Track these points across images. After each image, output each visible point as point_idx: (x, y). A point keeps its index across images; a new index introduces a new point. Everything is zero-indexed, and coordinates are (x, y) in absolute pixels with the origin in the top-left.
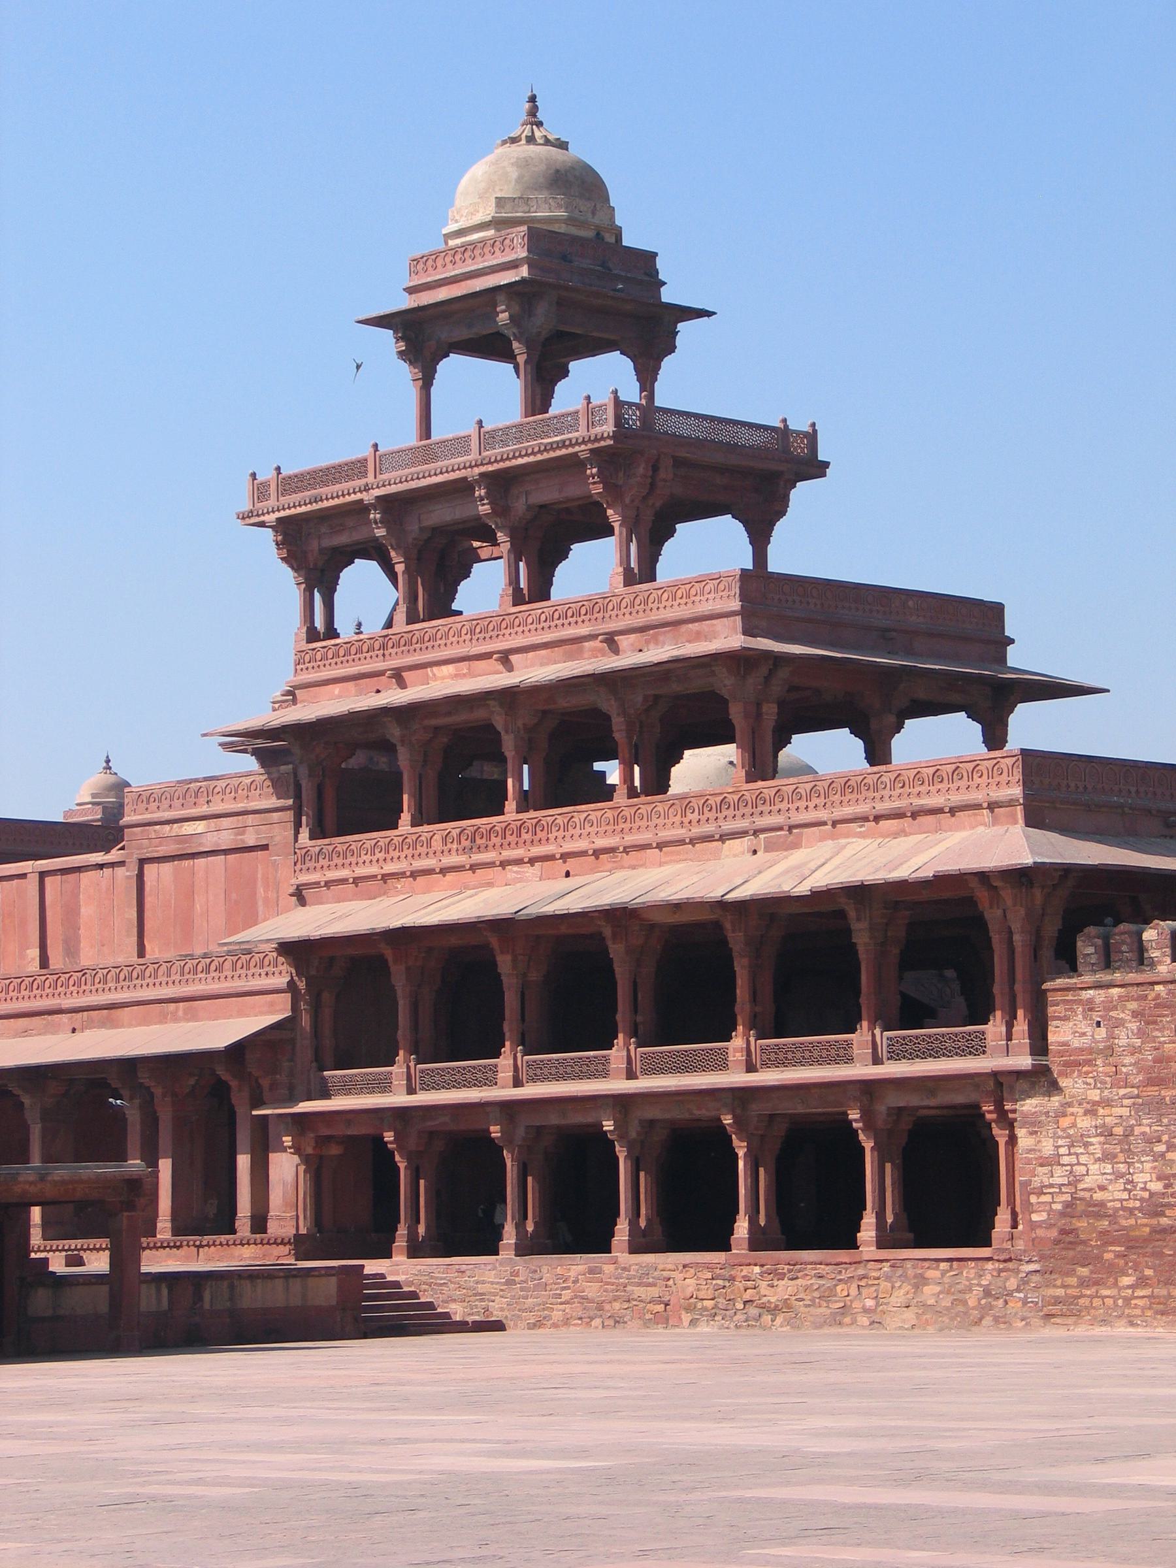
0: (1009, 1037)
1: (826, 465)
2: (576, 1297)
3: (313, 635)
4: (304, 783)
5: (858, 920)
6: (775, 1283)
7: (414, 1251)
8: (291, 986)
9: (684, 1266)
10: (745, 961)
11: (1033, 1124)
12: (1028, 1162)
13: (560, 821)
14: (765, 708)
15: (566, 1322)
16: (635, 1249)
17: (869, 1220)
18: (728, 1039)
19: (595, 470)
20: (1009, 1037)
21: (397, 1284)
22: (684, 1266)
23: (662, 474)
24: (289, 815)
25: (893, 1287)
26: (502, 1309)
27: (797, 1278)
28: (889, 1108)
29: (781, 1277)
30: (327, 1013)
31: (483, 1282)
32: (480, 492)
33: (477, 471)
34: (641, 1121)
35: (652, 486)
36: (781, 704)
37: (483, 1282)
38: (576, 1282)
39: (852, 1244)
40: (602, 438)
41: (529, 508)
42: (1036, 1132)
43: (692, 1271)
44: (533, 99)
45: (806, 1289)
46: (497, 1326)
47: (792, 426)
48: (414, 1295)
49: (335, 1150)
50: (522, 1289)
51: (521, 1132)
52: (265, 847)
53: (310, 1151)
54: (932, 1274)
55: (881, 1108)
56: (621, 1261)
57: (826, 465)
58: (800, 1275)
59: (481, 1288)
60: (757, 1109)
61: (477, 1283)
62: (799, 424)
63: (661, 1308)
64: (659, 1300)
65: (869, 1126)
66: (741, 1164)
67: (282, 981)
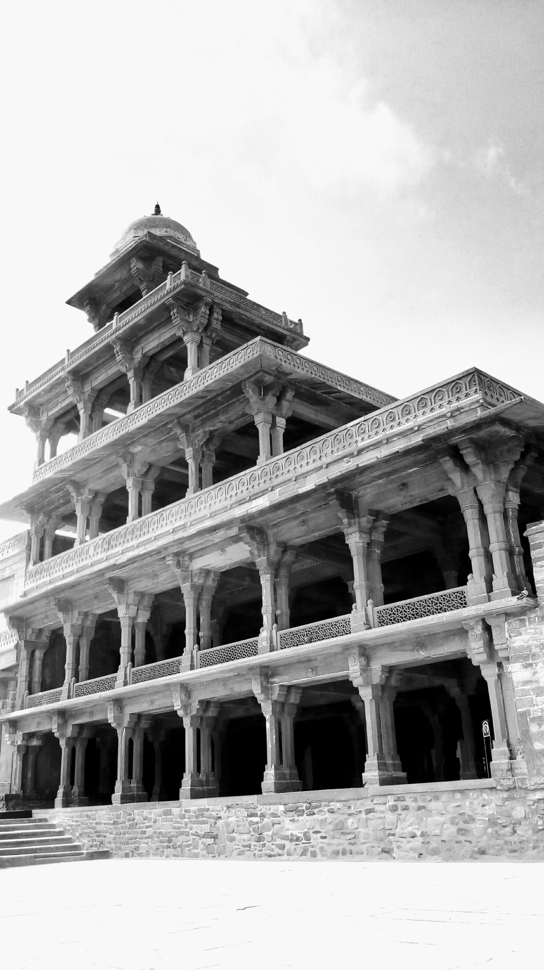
0: (490, 589)
1: (308, 339)
2: (155, 833)
3: (41, 460)
4: (33, 537)
5: (350, 525)
6: (296, 818)
7: (67, 804)
8: (17, 647)
9: (228, 807)
10: (268, 576)
11: (526, 658)
12: (526, 693)
13: (155, 518)
14: (278, 419)
15: (148, 854)
16: (195, 795)
17: (371, 760)
18: (257, 634)
19: (175, 310)
20: (490, 589)
21: (53, 826)
22: (228, 807)
23: (215, 315)
24: (24, 555)
25: (398, 819)
26: (110, 843)
27: (314, 814)
28: (383, 667)
29: (301, 813)
30: (38, 664)
31: (100, 823)
32: (117, 348)
33: (114, 336)
34: (201, 702)
35: (209, 321)
36: (289, 421)
37: (100, 823)
38: (155, 822)
39: (359, 783)
40: (178, 286)
41: (144, 355)
42: (531, 665)
43: (233, 811)
44: (158, 207)
45: (323, 822)
46: (105, 855)
47: (290, 317)
48: (60, 833)
49: (35, 742)
50: (122, 828)
51: (127, 719)
52: (12, 576)
53: (19, 743)
54: (433, 805)
55: (376, 667)
56: (187, 804)
57: (308, 339)
58: (316, 811)
59: (99, 828)
60: (279, 681)
61: (97, 824)
62: (293, 317)
63: (211, 841)
64: (207, 835)
65: (367, 683)
66: (268, 725)
67: (12, 645)
